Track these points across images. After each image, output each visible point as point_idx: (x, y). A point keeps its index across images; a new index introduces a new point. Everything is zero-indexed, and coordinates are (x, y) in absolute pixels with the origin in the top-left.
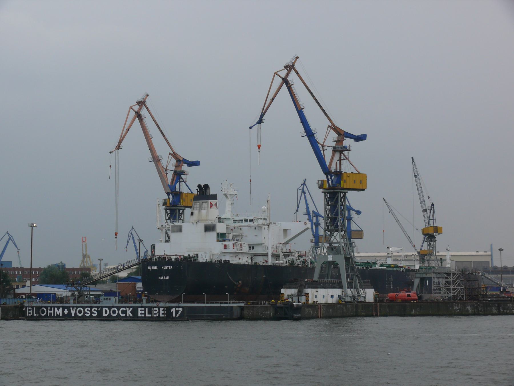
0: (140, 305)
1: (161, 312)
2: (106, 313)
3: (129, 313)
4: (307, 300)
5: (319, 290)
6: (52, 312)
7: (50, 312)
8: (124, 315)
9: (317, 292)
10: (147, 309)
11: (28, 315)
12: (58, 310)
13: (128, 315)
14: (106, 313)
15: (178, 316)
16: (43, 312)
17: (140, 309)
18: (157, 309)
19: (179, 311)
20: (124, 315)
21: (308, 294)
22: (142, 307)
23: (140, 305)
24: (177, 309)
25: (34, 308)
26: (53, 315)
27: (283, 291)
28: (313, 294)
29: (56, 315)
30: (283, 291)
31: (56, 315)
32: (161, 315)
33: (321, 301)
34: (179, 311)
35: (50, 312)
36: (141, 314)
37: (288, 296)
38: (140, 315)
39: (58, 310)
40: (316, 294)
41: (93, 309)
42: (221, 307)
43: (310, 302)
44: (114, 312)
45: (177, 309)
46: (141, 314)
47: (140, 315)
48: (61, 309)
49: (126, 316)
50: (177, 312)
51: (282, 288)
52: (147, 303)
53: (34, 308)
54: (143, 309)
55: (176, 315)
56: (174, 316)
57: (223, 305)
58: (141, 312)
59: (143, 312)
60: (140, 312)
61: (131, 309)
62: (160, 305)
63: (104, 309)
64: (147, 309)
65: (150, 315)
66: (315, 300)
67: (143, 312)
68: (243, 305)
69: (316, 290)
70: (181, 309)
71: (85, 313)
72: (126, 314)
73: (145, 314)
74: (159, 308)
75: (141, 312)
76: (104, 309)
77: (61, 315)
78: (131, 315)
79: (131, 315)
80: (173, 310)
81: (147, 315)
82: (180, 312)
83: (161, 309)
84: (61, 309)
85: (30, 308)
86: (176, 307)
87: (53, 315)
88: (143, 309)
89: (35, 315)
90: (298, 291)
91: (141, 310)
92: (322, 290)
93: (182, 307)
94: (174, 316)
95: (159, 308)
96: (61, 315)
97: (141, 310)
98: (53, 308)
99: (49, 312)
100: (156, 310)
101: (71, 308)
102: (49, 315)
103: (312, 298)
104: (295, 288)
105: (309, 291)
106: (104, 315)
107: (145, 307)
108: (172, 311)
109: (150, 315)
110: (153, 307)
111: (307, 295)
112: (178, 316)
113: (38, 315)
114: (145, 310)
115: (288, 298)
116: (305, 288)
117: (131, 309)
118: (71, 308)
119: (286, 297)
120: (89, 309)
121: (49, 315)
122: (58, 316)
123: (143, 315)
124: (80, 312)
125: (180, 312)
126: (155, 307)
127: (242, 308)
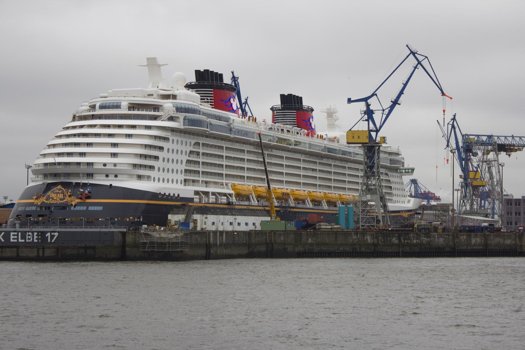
0: (13, 230)
1: (35, 237)
4: (195, 227)
5: (209, 216)
9: (206, 218)
10: (20, 233)
15: (53, 241)
17: (12, 234)
18: (30, 234)
19: (54, 236)
21: (196, 220)
22: (15, 231)
23: (13, 230)
24: (53, 234)
27: (170, 217)
28: (202, 221)
30: (170, 217)
32: (35, 241)
33: (210, 228)
34: (54, 236)
36: (13, 239)
37: (176, 222)
38: (12, 240)
40: (206, 220)
42: (100, 232)
43: (199, 229)
45: (53, 234)
46: (13, 239)
47: (12, 240)
50: (52, 237)
51: (169, 213)
52: (20, 227)
55: (51, 239)
56: (49, 241)
57: (102, 230)
58: (13, 237)
59: (16, 237)
60: (12, 237)
61: (3, 233)
62: (34, 230)
64: (20, 233)
65: (23, 241)
66: (204, 226)
67: (16, 237)
68: (125, 230)
69: (205, 216)
70: (56, 234)
73: (18, 239)
74: (33, 233)
75: (13, 237)
78: (3, 240)
81: (20, 240)
82: (55, 237)
83: (35, 234)
86: (51, 232)
88: (16, 233)
90: (186, 217)
91: (13, 235)
92: (212, 216)
93: (58, 232)
94: (49, 241)
95: (33, 233)
97: (13, 235)
100: (29, 235)
103: (201, 225)
104: (183, 214)
105: (197, 217)
107: (18, 232)
108: (47, 235)
109: (23, 241)
110: (26, 232)
111: (195, 221)
112: (53, 241)
114: (18, 235)
115: (176, 224)
116: (193, 214)
117: (3, 233)
119: (173, 223)
123: (16, 241)
125: (55, 237)
126: (29, 232)
127: (124, 234)
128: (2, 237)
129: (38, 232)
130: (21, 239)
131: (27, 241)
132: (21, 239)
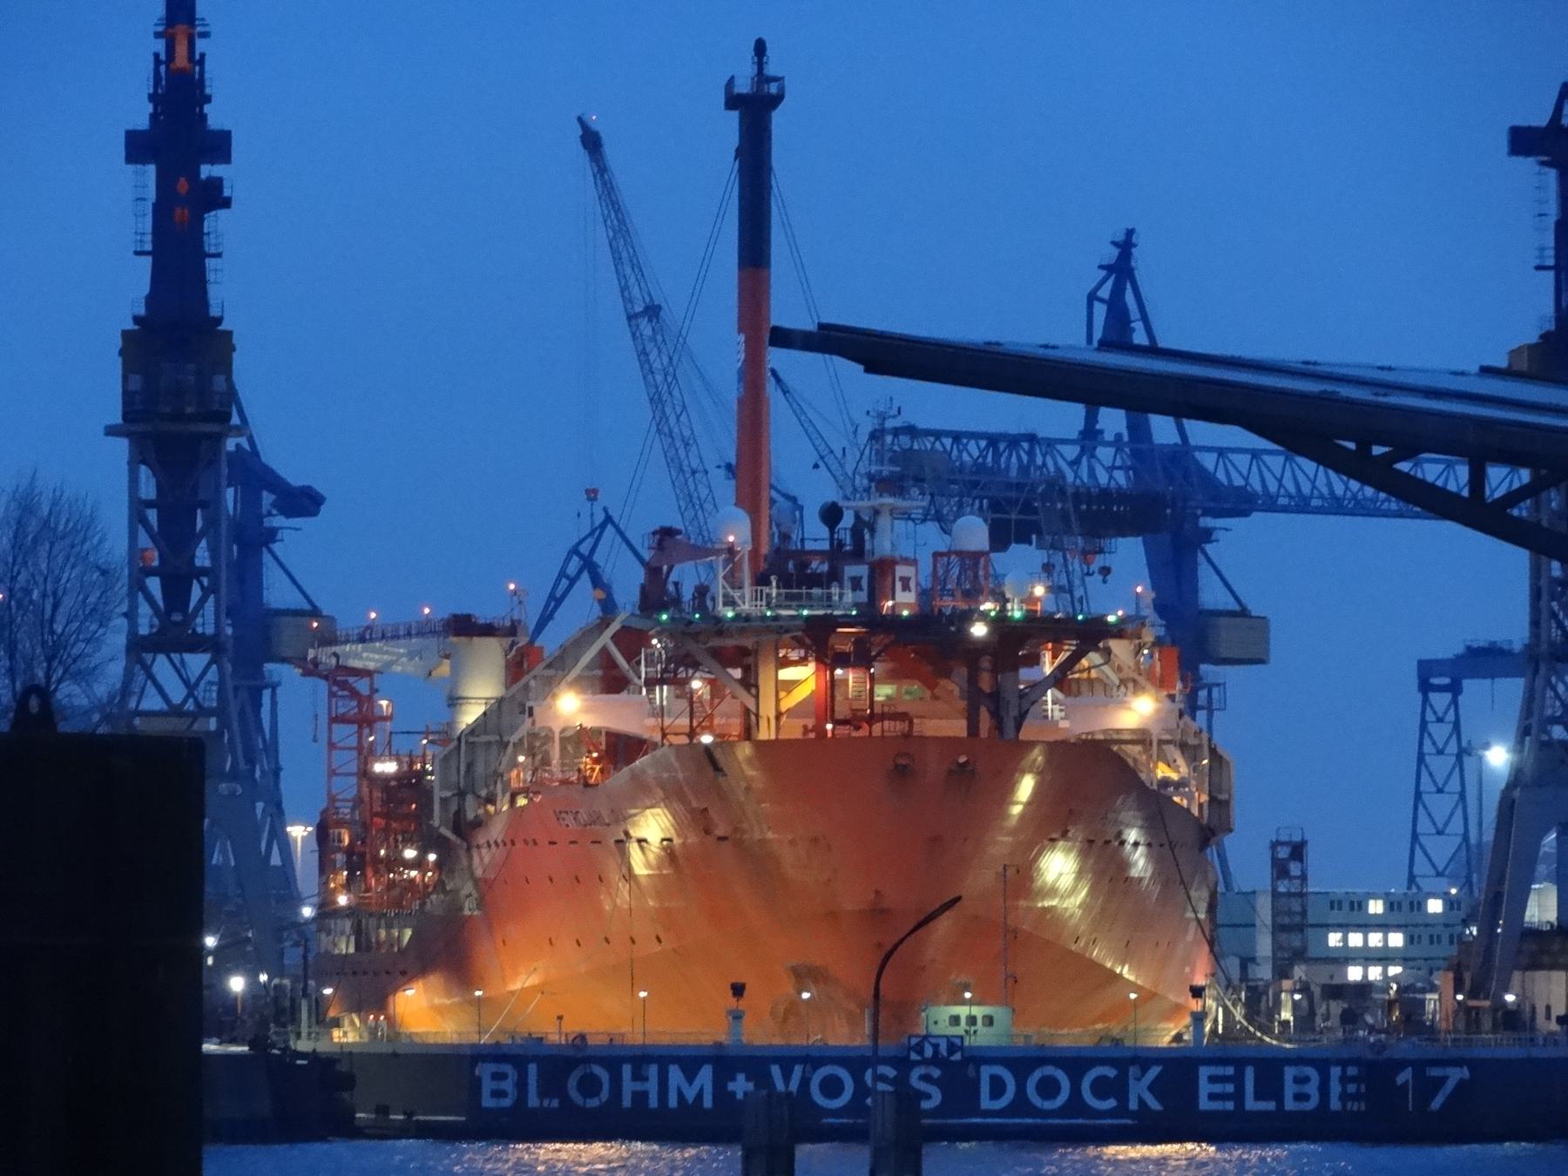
1: (1335, 1088)
2: (997, 1088)
3: (1140, 1091)
6: (652, 1086)
7: (639, 1086)
8: (1111, 1103)
10: (1250, 1073)
11: (488, 1102)
12: (690, 1078)
13: (1133, 1105)
14: (997, 1088)
15: (1436, 1104)
16: (590, 1086)
17: (1204, 1072)
18: (1311, 1072)
20: (1111, 1103)
24: (1435, 1072)
25: (532, 1069)
26: (653, 1102)
29: (673, 1102)
31: (673, 1102)
34: (1442, 1080)
35: (639, 1086)
36: (1212, 1097)
38: (1205, 1104)
39: (690, 1078)
41: (915, 1074)
44: (1048, 1088)
45: (1435, 1072)
46: (1212, 1097)
47: (1205, 1104)
48: (706, 1075)
49: (1121, 1110)
53: (532, 1069)
54: (1230, 1071)
58: (1217, 1088)
59: (1230, 1088)
60: (1205, 1088)
61: (1154, 1071)
63: (986, 1072)
64: (1250, 1073)
65: (1270, 1106)
67: (1230, 1088)
70: (1456, 1075)
71: (861, 1091)
72: (1123, 1098)
73: (1239, 1096)
75: (1217, 1088)
76: (986, 1072)
77: (708, 1103)
78: (1154, 1105)
79: (1154, 1105)
80: (1405, 1076)
81: (1251, 1104)
82: (1450, 1085)
83: (1335, 1072)
84: (706, 1075)
85: (508, 1068)
87: (653, 1102)
88: (1230, 1071)
89: (533, 1101)
91: (1213, 1079)
96: (708, 1103)
97: (1213, 1079)
98: (653, 1071)
99: (629, 1086)
101: (776, 1071)
102: (627, 1102)
106: (986, 1103)
109: (1270, 1106)
112: (1436, 1104)
113: (555, 1103)
114: (1238, 1079)
117: (1154, 1071)
118: (776, 1071)
120: (890, 1072)
121: (627, 1102)
122: (690, 1109)
123: (1230, 1106)
124: (832, 1087)
128: (1151, 1088)
129: (1344, 1063)
130: (1258, 1096)
131: (1290, 1105)
132: (1258, 1096)
